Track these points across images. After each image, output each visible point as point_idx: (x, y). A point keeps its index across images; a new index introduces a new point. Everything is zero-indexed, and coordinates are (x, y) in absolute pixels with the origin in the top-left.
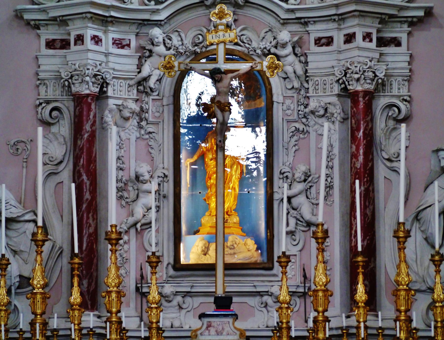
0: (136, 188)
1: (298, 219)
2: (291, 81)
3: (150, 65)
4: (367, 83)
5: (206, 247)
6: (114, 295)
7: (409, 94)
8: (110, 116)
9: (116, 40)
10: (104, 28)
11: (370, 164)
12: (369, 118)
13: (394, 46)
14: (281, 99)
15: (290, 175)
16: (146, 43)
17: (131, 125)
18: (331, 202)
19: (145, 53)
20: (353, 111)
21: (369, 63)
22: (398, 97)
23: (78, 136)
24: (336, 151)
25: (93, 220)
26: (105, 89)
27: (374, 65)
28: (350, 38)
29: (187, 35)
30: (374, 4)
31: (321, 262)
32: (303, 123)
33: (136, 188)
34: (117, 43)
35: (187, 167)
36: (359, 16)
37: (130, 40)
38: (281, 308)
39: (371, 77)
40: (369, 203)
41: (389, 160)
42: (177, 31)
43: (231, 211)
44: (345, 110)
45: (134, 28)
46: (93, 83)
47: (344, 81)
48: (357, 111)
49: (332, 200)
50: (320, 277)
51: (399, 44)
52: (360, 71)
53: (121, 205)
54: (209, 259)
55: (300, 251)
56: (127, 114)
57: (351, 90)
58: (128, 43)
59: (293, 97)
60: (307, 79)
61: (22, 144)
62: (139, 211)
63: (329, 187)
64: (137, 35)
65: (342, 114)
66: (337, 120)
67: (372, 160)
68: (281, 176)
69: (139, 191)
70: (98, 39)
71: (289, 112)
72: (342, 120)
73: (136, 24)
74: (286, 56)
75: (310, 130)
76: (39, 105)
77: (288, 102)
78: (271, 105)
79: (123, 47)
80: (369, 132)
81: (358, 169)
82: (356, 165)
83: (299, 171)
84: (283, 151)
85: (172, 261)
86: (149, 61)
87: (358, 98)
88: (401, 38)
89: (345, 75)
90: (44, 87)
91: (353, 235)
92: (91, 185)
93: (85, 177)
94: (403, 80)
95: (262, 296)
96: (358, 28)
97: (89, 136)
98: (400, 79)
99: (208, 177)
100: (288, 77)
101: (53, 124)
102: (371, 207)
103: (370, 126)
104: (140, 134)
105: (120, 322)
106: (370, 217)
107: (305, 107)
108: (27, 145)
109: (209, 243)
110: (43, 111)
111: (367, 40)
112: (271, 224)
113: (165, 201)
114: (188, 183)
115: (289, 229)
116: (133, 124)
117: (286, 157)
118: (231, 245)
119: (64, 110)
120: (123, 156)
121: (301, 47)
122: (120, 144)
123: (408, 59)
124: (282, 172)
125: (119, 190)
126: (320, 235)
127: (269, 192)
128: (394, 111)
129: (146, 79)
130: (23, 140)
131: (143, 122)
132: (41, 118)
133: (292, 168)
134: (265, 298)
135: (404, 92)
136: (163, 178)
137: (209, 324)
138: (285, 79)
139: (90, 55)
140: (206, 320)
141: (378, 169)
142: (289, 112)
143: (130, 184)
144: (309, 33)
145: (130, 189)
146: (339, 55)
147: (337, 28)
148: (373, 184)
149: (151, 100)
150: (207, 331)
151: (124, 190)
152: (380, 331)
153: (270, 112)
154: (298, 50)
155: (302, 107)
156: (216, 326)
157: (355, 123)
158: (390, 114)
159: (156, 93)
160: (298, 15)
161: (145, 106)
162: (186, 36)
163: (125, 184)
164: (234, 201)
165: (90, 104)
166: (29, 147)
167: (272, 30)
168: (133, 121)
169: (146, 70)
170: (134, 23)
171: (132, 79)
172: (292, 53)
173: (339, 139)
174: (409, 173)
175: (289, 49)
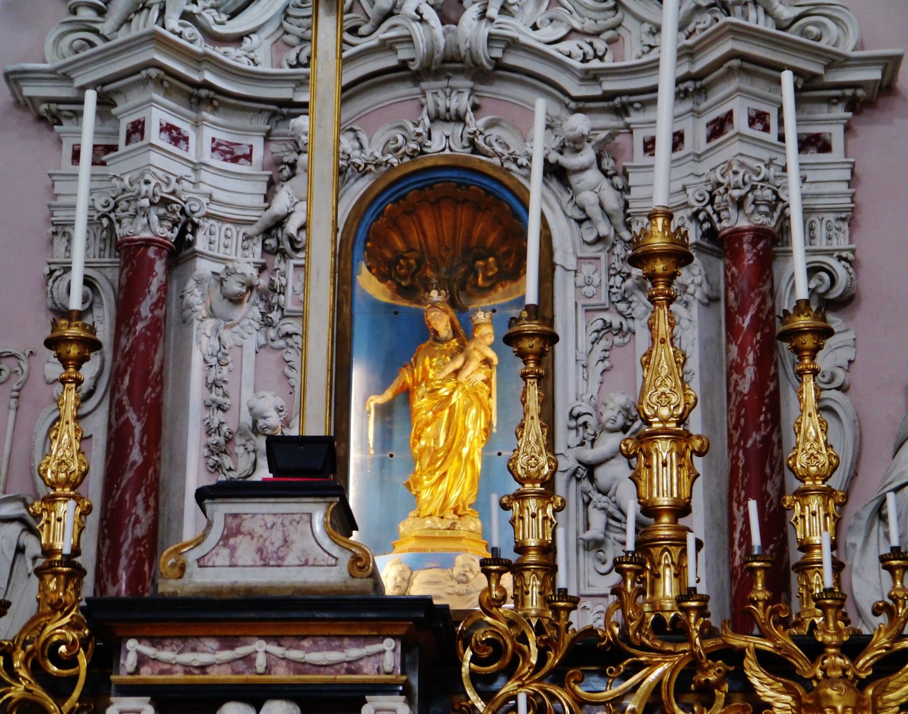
0: (251, 448)
1: (610, 516)
2: (594, 225)
3: (290, 192)
4: (760, 213)
5: (403, 579)
7: (853, 246)
9: (219, 144)
10: (192, 114)
11: (772, 386)
12: (766, 288)
13: (815, 151)
14: (571, 263)
15: (592, 421)
16: (283, 148)
17: (245, 317)
19: (281, 171)
20: (729, 274)
21: (764, 171)
22: (829, 253)
23: (122, 329)
25: (147, 508)
26: (189, 237)
27: (775, 176)
28: (719, 127)
29: (374, 138)
30: (771, 42)
31: (663, 341)
32: (620, 313)
33: (251, 448)
34: (222, 151)
35: (369, 412)
36: (741, 69)
37: (251, 146)
38: (520, 496)
39: (770, 199)
40: (772, 469)
42: (352, 130)
43: (464, 508)
44: (711, 280)
45: (262, 124)
46: (161, 218)
47: (708, 215)
48: (740, 272)
50: (662, 389)
51: (825, 147)
52: (745, 184)
56: (234, 286)
57: (725, 228)
58: (248, 152)
59: (598, 259)
60: (628, 220)
61: (12, 361)
64: (267, 138)
65: (705, 288)
66: (695, 298)
67: (776, 375)
68: (573, 423)
69: (258, 453)
70: (179, 134)
71: (589, 290)
72: (706, 301)
73: (266, 114)
74: (583, 170)
77: (587, 269)
78: (550, 271)
79: (235, 160)
80: (767, 317)
81: (746, 395)
82: (740, 388)
83: (611, 405)
84: (577, 371)
86: (287, 186)
87: (741, 244)
88: (830, 135)
89: (712, 202)
90: (64, 240)
91: (736, 543)
92: (144, 431)
93: (132, 416)
94: (838, 219)
96: (738, 99)
97: (146, 328)
98: (831, 217)
99: (415, 437)
100: (588, 219)
102: (777, 480)
103: (769, 304)
104: (266, 339)
106: (775, 501)
108: (22, 363)
109: (412, 570)
110: (56, 285)
111: (759, 126)
114: (371, 446)
115: (588, 535)
116: (250, 315)
117: (582, 384)
118: (460, 575)
120: (225, 382)
121: (615, 160)
122: (220, 355)
123: (847, 175)
124: (575, 413)
128: (821, 279)
129: (280, 222)
130: (14, 351)
131: (275, 313)
132: (54, 307)
133: (596, 408)
135: (841, 242)
137: (234, 523)
138: (580, 222)
139: (155, 158)
141: (787, 406)
142: (589, 290)
143: (238, 440)
144: (631, 133)
145: (240, 450)
146: (696, 164)
147: (692, 111)
148: (779, 431)
149: (292, 267)
150: (225, 552)
151: (225, 452)
152: (894, 562)
153: (548, 285)
154: (608, 163)
155: (618, 279)
156: (259, 530)
157: (736, 299)
159: (302, 255)
160: (610, 85)
161: (278, 280)
162: (370, 141)
163: (228, 441)
164: (471, 488)
165: (152, 262)
166: (25, 366)
167: (553, 124)
168: (250, 310)
169: (282, 201)
170: (261, 111)
171: (251, 223)
172: (595, 165)
173: (700, 338)
174: (857, 414)
175: (588, 155)
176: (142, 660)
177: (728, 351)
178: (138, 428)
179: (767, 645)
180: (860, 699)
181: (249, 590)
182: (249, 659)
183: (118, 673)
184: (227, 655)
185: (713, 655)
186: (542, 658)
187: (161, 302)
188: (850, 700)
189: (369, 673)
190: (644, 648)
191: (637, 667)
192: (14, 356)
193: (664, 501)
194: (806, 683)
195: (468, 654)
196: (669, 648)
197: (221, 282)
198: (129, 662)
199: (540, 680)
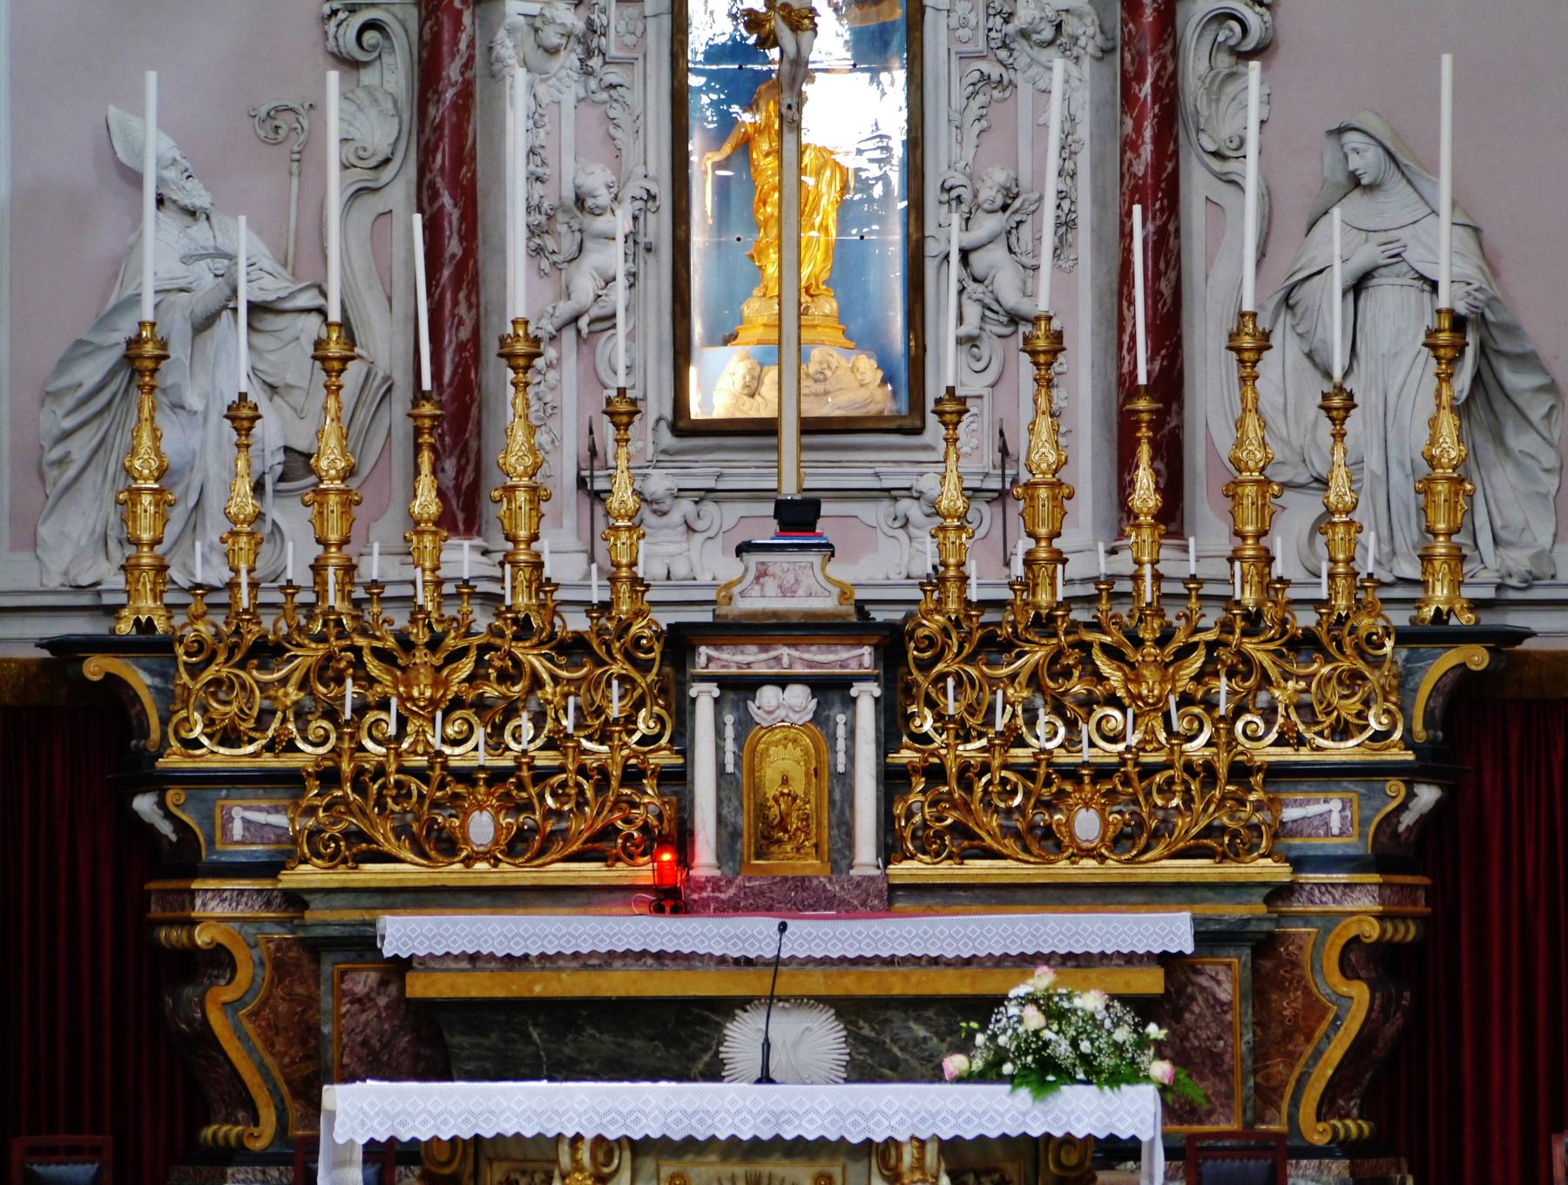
0: (576, 227)
5: (753, 378)
6: (521, 497)
8: (509, 43)
11: (1170, 166)
12: (1167, 49)
15: (966, 194)
17: (562, 67)
18: (1071, 263)
20: (1126, 30)
23: (430, 94)
24: (1083, 131)
25: (470, 307)
31: (1044, 413)
32: (1001, 62)
33: (576, 227)
35: (705, 172)
38: (943, 529)
41: (1216, 154)
43: (818, 287)
44: (1106, 26)
48: (1137, 31)
49: (1072, 257)
50: (1043, 450)
53: (540, 270)
54: (762, 408)
55: (993, 386)
56: (552, 37)
61: (290, 116)
62: (584, 285)
65: (1099, 39)
66: (1086, 53)
67: (1176, 154)
68: (945, 197)
69: (585, 234)
71: (964, 33)
72: (1100, 54)
75: (1019, 78)
76: (330, 17)
78: (919, 16)
80: (1167, 85)
81: (1140, 178)
82: (1135, 169)
83: (989, 183)
84: (950, 132)
85: (668, 412)
91: (1125, 347)
92: (462, 219)
93: (446, 199)
95: (895, 499)
97: (457, 95)
99: (759, 200)
101: (366, 64)
102: (1172, 275)
103: (1170, 68)
104: (586, 91)
105: (538, 565)
106: (1169, 301)
107: (1006, 21)
108: (301, 119)
109: (762, 365)
112: (918, 317)
113: (651, 258)
115: (964, 330)
116: (568, 64)
117: (956, 149)
118: (817, 373)
119: (394, 28)
120: (543, 147)
122: (536, 116)
124: (947, 185)
125: (533, 231)
126: (1042, 344)
127: (914, 237)
128: (1231, 30)
130: (291, 105)
131: (595, 59)
132: (335, 50)
133: (971, 177)
134: (905, 505)
136: (646, 201)
137: (762, 568)
140: (753, 559)
141: (1189, 177)
142: (964, 33)
143: (561, 217)
145: (563, 229)
148: (1177, 217)
150: (757, 588)
151: (547, 232)
152: (1192, 586)
153: (917, 34)
155: (999, 20)
156: (779, 573)
158: (1221, 38)
161: (599, 19)
163: (549, 217)
164: (824, 260)
165: (459, 14)
166: (305, 124)
168: (567, 57)
173: (1092, 102)
174: (1267, 187)
176: (710, 659)
177: (1122, 123)
178: (456, 214)
179: (1108, 639)
181: (775, 614)
182: (778, 659)
183: (694, 667)
184: (764, 656)
186: (961, 647)
187: (469, 63)
188: (1158, 676)
189: (853, 669)
191: (1026, 653)
192: (291, 109)
194: (1132, 666)
195: (912, 645)
196: (1044, 642)
197: (536, 30)
198: (702, 660)
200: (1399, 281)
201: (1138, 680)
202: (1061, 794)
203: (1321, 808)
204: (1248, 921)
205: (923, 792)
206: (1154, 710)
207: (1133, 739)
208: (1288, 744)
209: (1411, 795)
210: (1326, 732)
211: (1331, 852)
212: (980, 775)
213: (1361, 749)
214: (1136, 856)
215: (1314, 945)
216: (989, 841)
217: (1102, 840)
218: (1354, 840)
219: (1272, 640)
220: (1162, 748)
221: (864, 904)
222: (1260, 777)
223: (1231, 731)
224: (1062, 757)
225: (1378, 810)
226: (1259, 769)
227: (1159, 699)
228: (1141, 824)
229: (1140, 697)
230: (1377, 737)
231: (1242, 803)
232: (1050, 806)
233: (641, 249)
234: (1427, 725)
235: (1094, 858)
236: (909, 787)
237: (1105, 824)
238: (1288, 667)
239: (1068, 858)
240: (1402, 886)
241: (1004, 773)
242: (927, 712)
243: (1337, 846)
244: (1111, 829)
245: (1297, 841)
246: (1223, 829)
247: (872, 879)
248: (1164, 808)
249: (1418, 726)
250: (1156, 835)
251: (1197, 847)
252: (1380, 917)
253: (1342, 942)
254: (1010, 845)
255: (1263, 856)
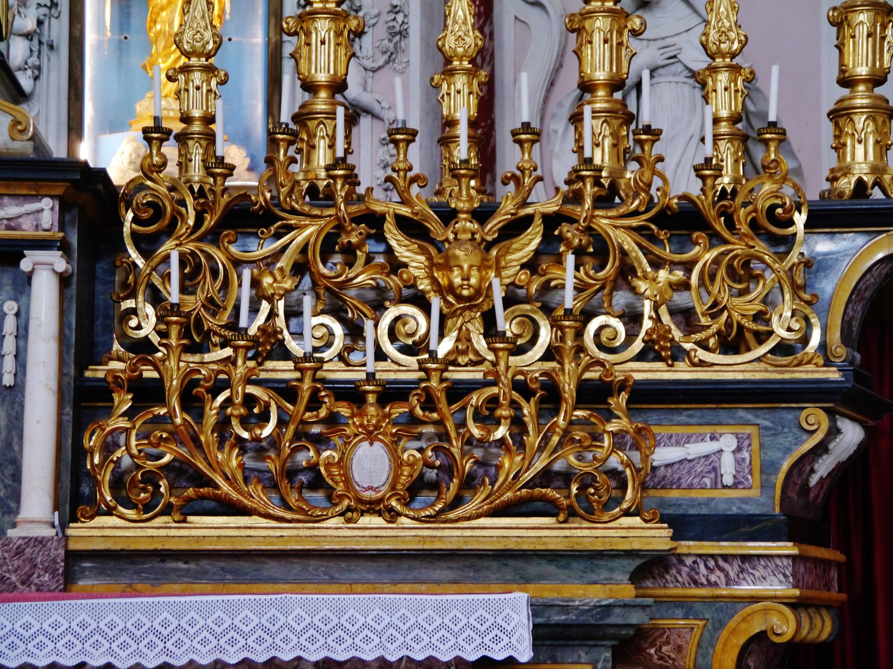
18: (404, 65)
38: (186, 70)
49: (405, 60)
63: (400, 33)
112: (275, 105)
113: (53, 57)
114: (108, 28)
127: (273, 40)
136: (50, 8)
148: (491, 23)
152: (523, 137)
179: (405, 211)
180: (485, 260)
185: (357, 220)
186: (199, 220)
188: (476, 259)
189: (27, 230)
190: (293, 212)
191: (290, 228)
193: (322, 77)
195: (130, 215)
196: (316, 212)
199: (200, 239)
200: (675, 79)
201: (447, 266)
202: (333, 420)
203: (708, 447)
204: (608, 609)
205: (130, 414)
206: (470, 308)
207: (444, 348)
208: (658, 358)
209: (834, 432)
210: (712, 342)
211: (722, 509)
212: (215, 392)
213: (762, 366)
214: (442, 511)
215: (699, 645)
216: (225, 487)
217: (393, 488)
218: (755, 493)
219: (635, 213)
220: (481, 361)
221: (26, 581)
222: (624, 397)
223: (579, 334)
224: (336, 372)
225: (788, 450)
226: (622, 386)
227: (478, 292)
228: (448, 470)
229: (451, 289)
230: (783, 349)
231: (596, 437)
232: (320, 441)
233: (45, 48)
234: (846, 339)
235: (380, 514)
236: (109, 411)
237: (397, 464)
238: (657, 250)
239: (342, 514)
240: (817, 561)
241: (251, 389)
242: (150, 310)
243: (730, 501)
244: (406, 471)
245: (674, 494)
246: (567, 477)
247: (40, 542)
248: (481, 442)
249: (835, 336)
250: (469, 483)
251: (531, 499)
252: (795, 605)
253: (742, 640)
254: (257, 496)
255: (627, 513)
